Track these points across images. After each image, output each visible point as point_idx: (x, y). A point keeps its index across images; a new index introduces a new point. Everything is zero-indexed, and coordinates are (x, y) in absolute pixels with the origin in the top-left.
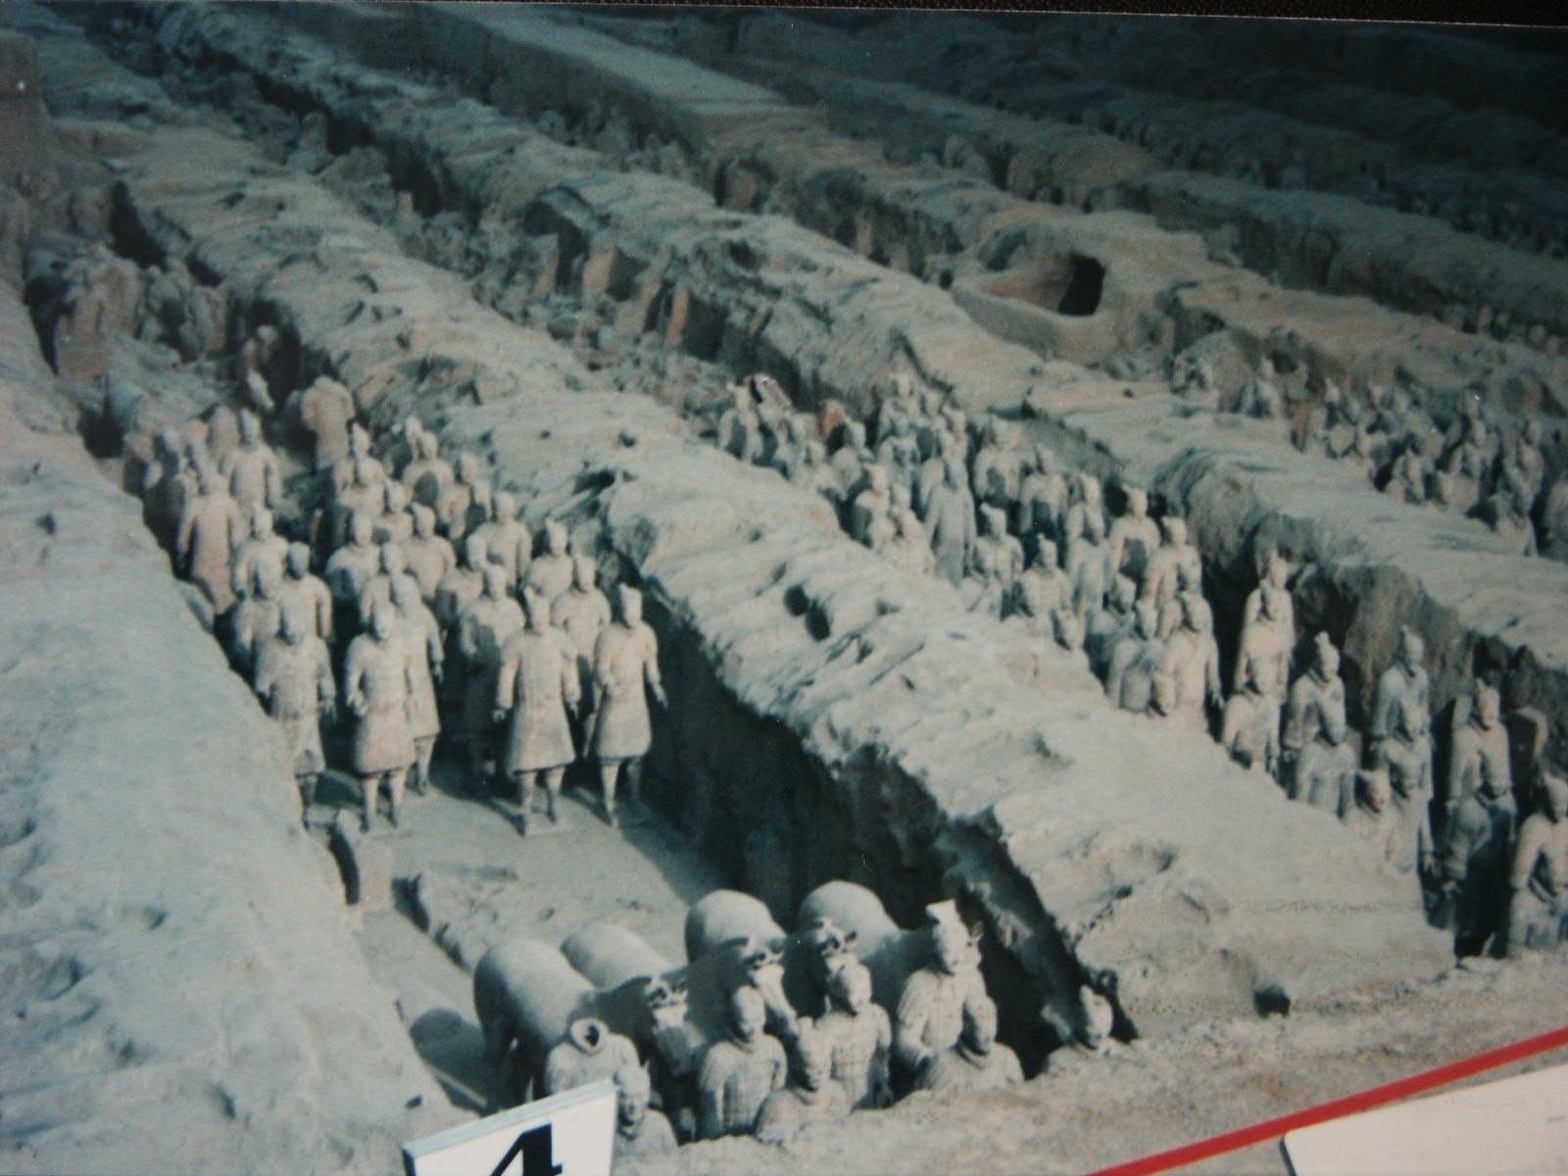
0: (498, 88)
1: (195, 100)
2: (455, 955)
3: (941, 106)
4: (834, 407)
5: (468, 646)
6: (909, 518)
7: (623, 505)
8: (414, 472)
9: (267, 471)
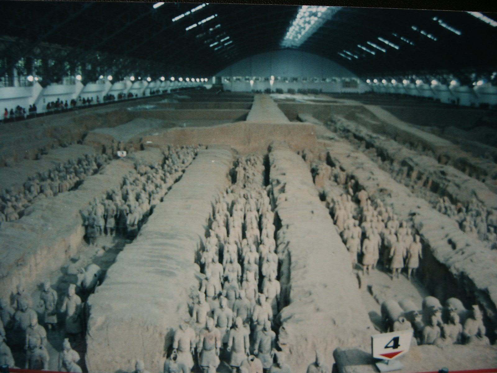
0: (397, 138)
1: (342, 137)
2: (377, 301)
3: (484, 146)
4: (459, 205)
5: (386, 243)
6: (474, 228)
7: (417, 219)
8: (378, 209)
9: (351, 207)
